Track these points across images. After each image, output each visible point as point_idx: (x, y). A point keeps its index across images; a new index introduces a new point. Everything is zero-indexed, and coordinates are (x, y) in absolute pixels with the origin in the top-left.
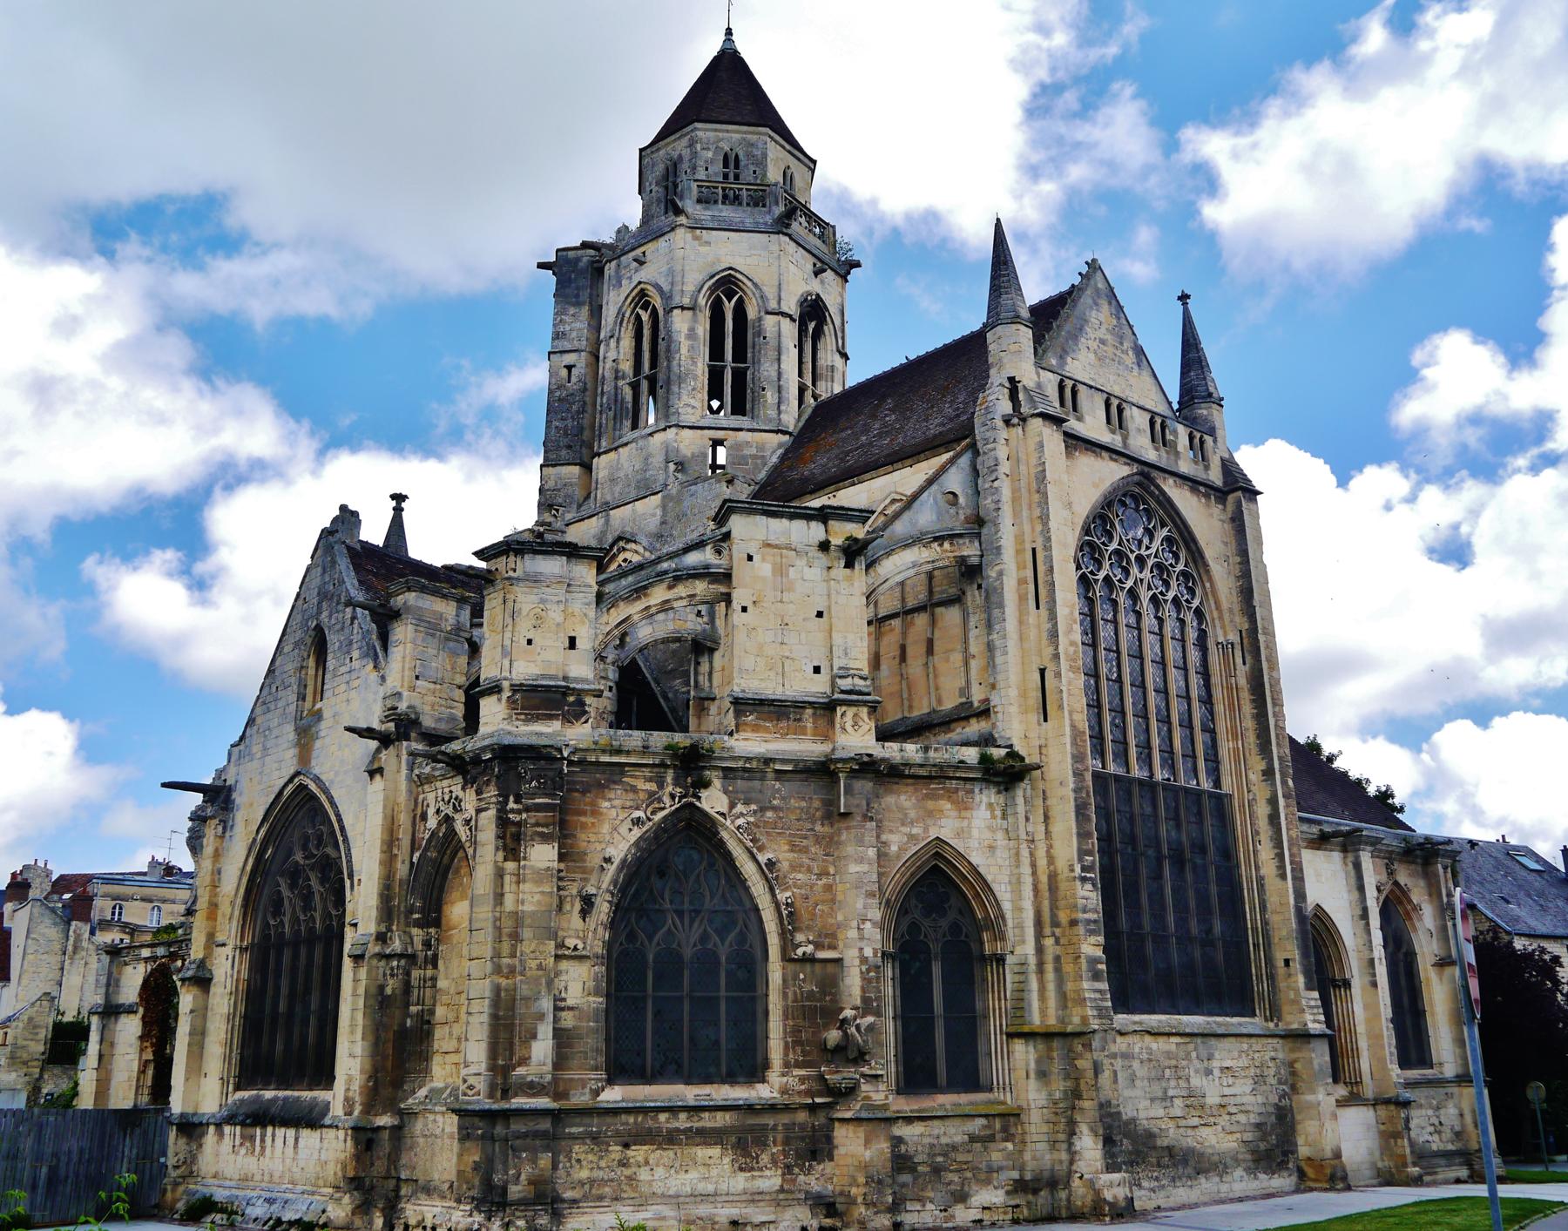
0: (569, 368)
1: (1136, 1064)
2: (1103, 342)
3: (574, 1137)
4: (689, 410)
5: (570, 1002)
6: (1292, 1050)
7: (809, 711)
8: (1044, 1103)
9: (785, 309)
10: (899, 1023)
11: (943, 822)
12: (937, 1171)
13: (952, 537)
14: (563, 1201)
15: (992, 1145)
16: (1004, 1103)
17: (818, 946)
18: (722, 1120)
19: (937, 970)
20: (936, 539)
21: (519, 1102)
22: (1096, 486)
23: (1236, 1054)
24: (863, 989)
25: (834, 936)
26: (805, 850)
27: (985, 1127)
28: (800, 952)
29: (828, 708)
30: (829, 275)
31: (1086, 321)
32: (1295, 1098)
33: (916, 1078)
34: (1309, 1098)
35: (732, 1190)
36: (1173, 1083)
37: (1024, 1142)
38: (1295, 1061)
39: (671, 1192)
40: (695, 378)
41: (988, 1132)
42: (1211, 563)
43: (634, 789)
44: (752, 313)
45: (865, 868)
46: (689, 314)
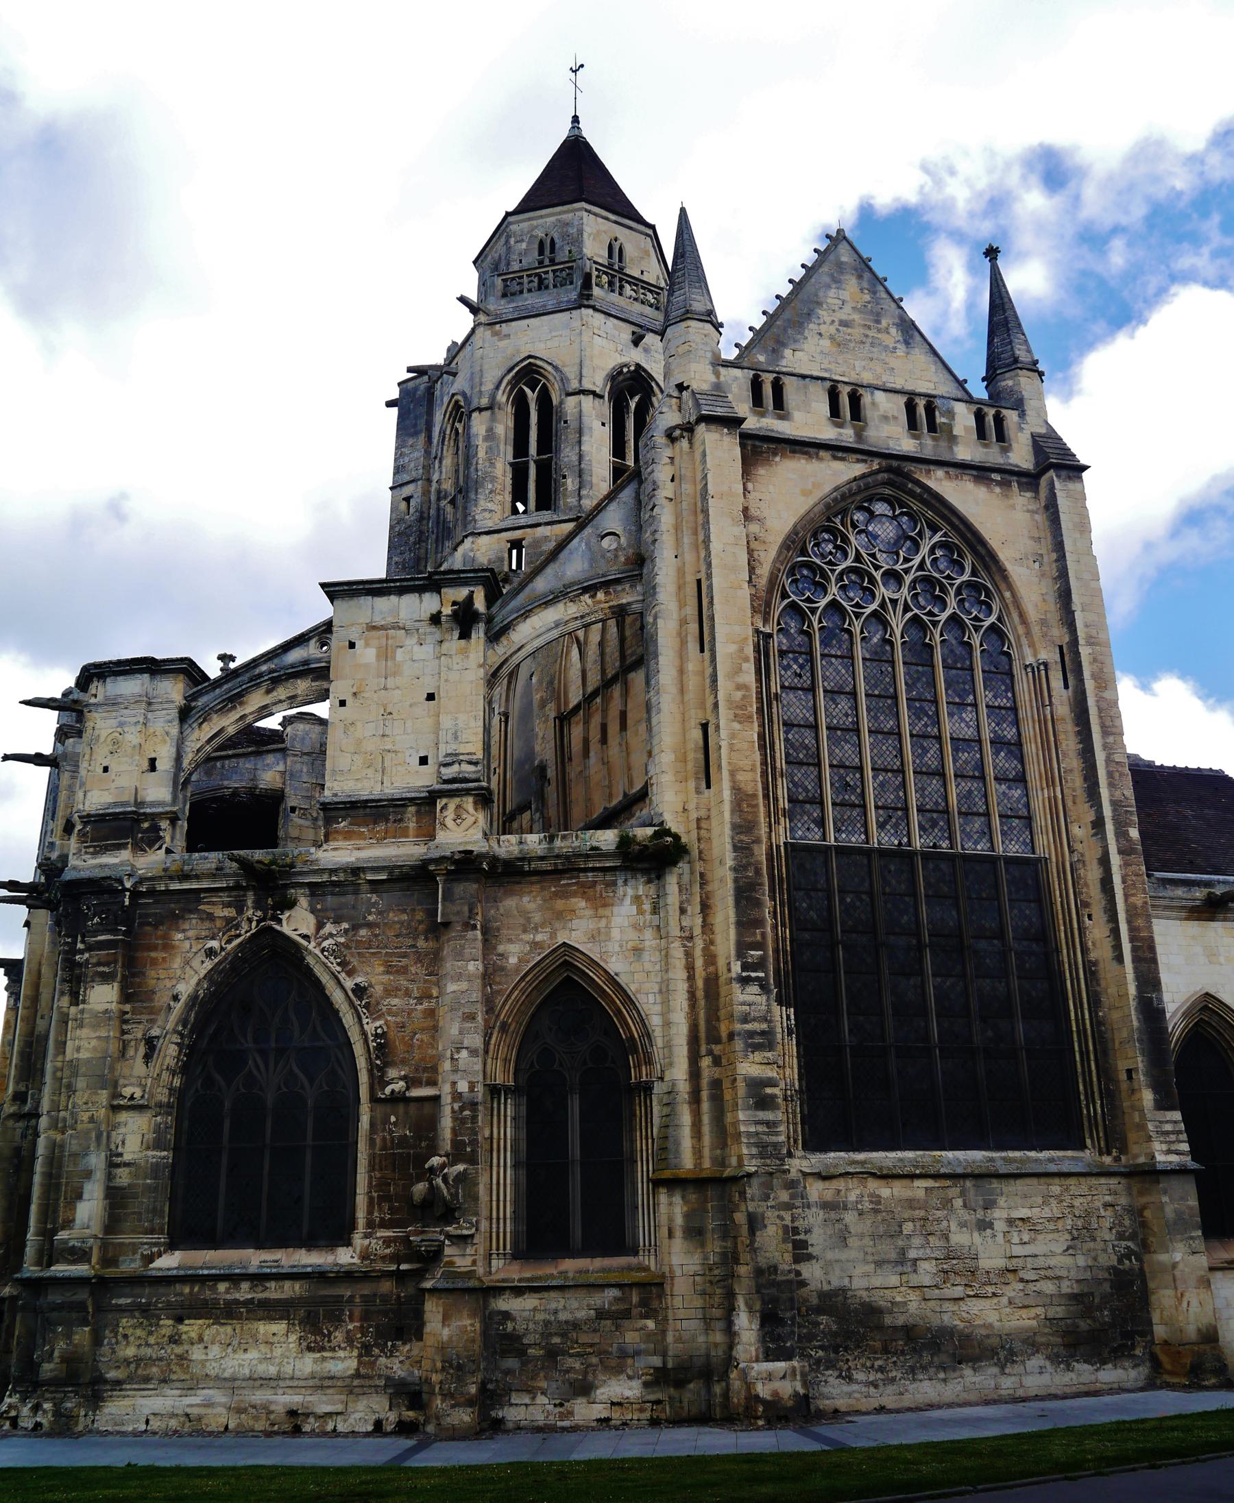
0: (407, 499)
1: (850, 1217)
2: (844, 324)
3: (121, 1310)
4: (487, 515)
5: (127, 1157)
6: (1141, 1193)
7: (412, 809)
8: (697, 1268)
9: (587, 385)
10: (523, 1173)
11: (575, 923)
12: (552, 1354)
13: (606, 585)
14: (106, 1381)
15: (626, 1323)
16: (647, 1269)
17: (411, 1082)
18: (291, 1290)
19: (575, 1106)
20: (585, 590)
21: (61, 1269)
22: (806, 493)
23: (1040, 1200)
24: (454, 1131)
25: (434, 1069)
26: (404, 971)
27: (617, 1299)
28: (388, 1090)
29: (428, 802)
30: (650, 339)
31: (819, 304)
32: (1146, 1257)
33: (540, 1235)
34: (1163, 1257)
35: (298, 1374)
36: (917, 1241)
37: (666, 1319)
38: (1144, 1207)
39: (226, 1375)
40: (493, 479)
41: (622, 1307)
42: (1009, 567)
43: (211, 917)
45: (464, 985)
46: (487, 414)
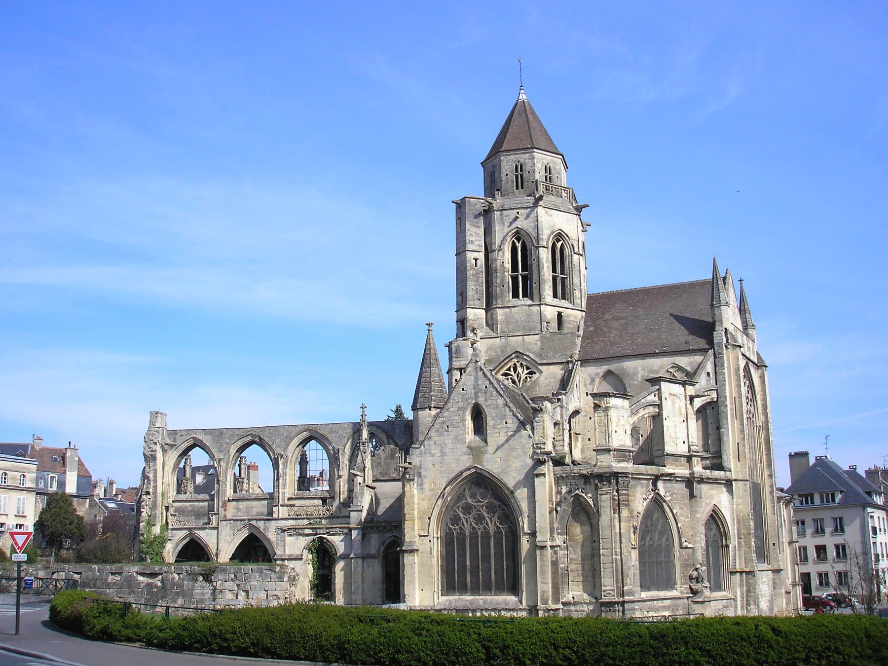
0: (476, 260)
29: (689, 458)
44: (567, 252)
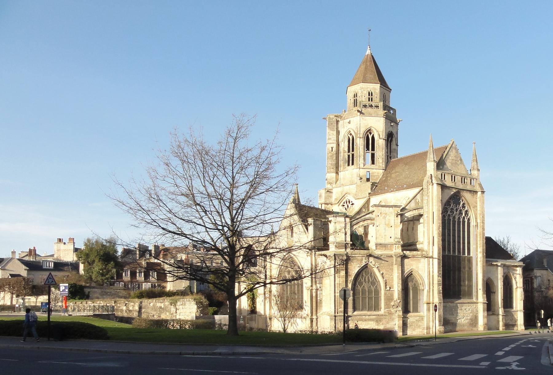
44: (376, 137)
